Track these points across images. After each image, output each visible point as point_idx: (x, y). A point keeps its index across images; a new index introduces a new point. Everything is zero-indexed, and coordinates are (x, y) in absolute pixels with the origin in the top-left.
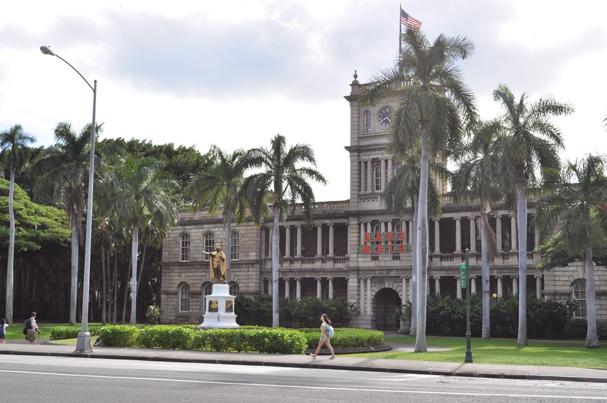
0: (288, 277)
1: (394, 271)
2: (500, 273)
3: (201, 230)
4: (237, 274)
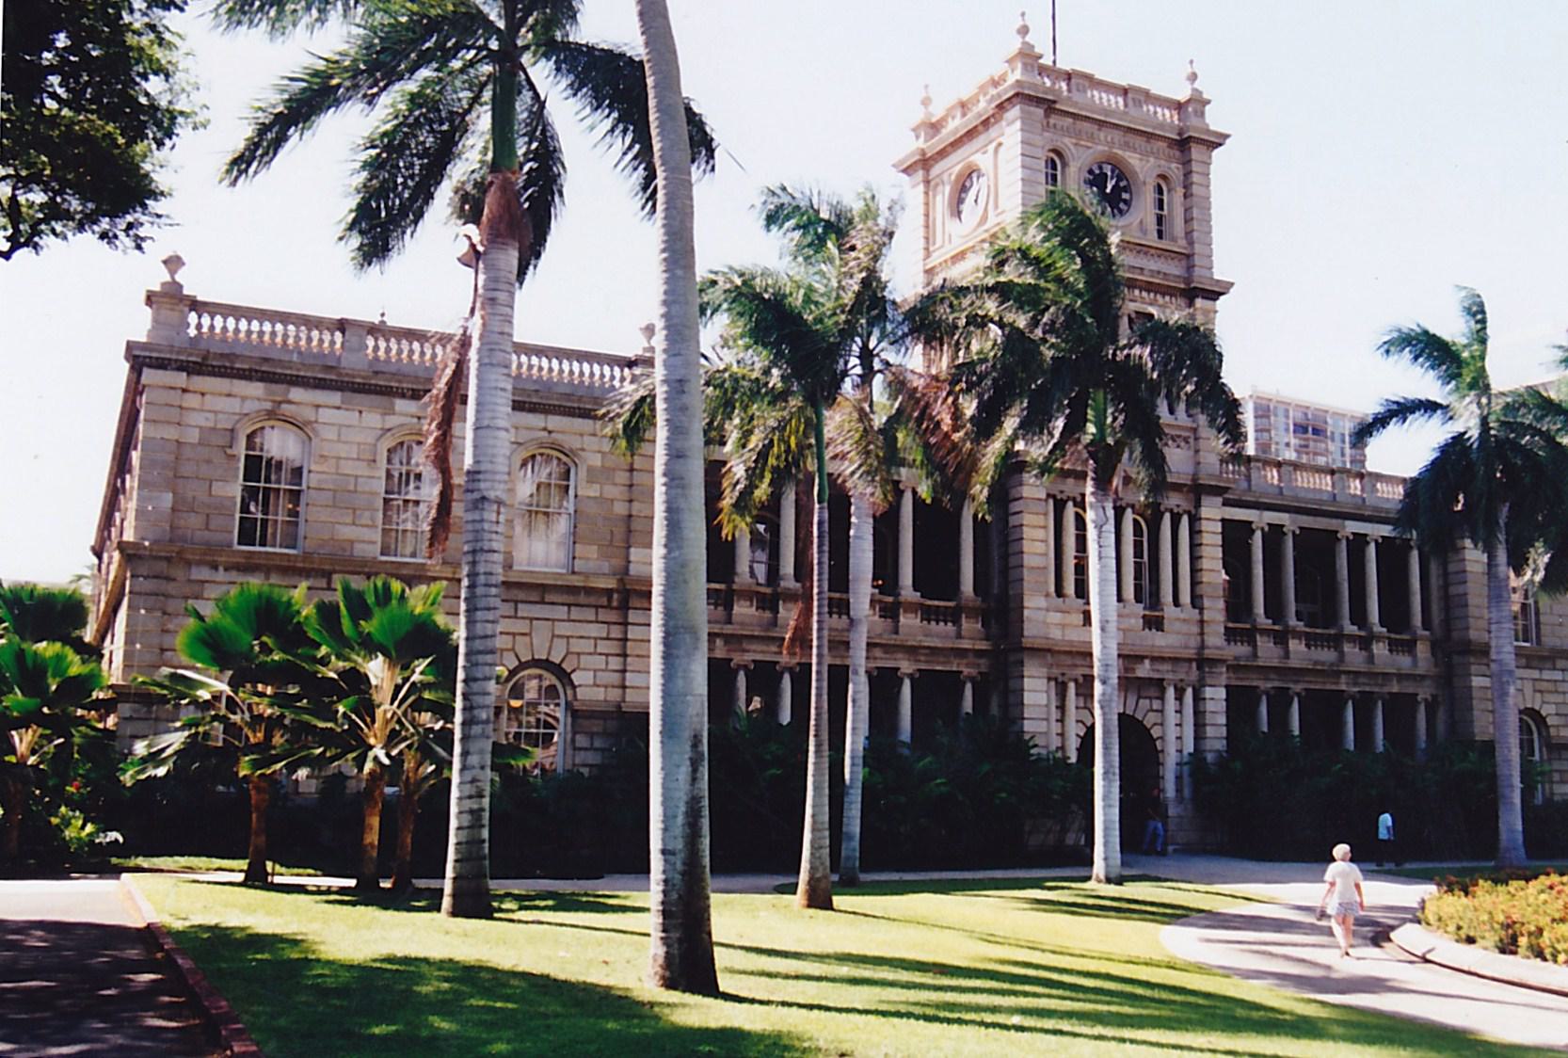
0: (749, 657)
1: (1147, 662)
2: (1355, 684)
3: (373, 419)
4: (563, 629)
